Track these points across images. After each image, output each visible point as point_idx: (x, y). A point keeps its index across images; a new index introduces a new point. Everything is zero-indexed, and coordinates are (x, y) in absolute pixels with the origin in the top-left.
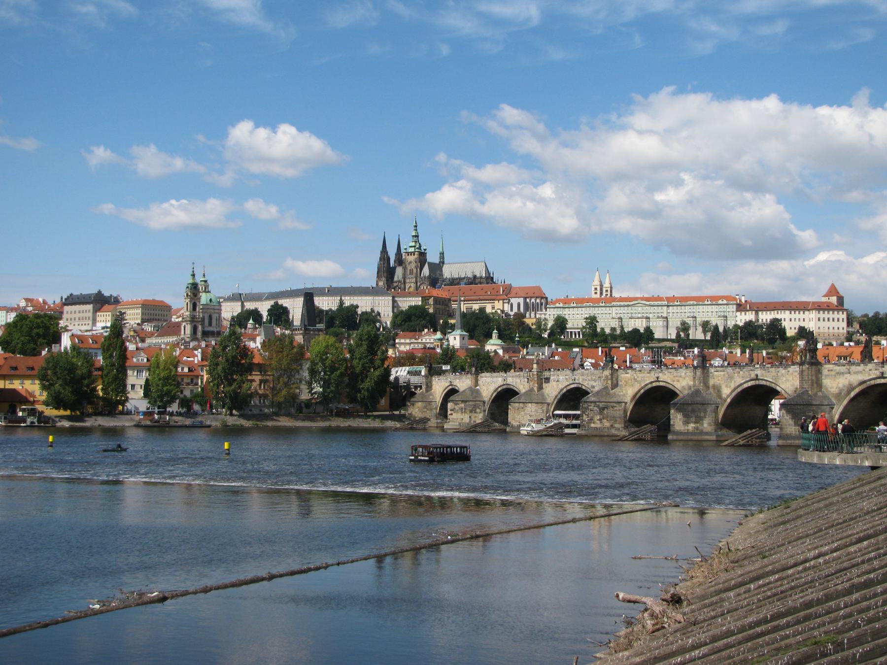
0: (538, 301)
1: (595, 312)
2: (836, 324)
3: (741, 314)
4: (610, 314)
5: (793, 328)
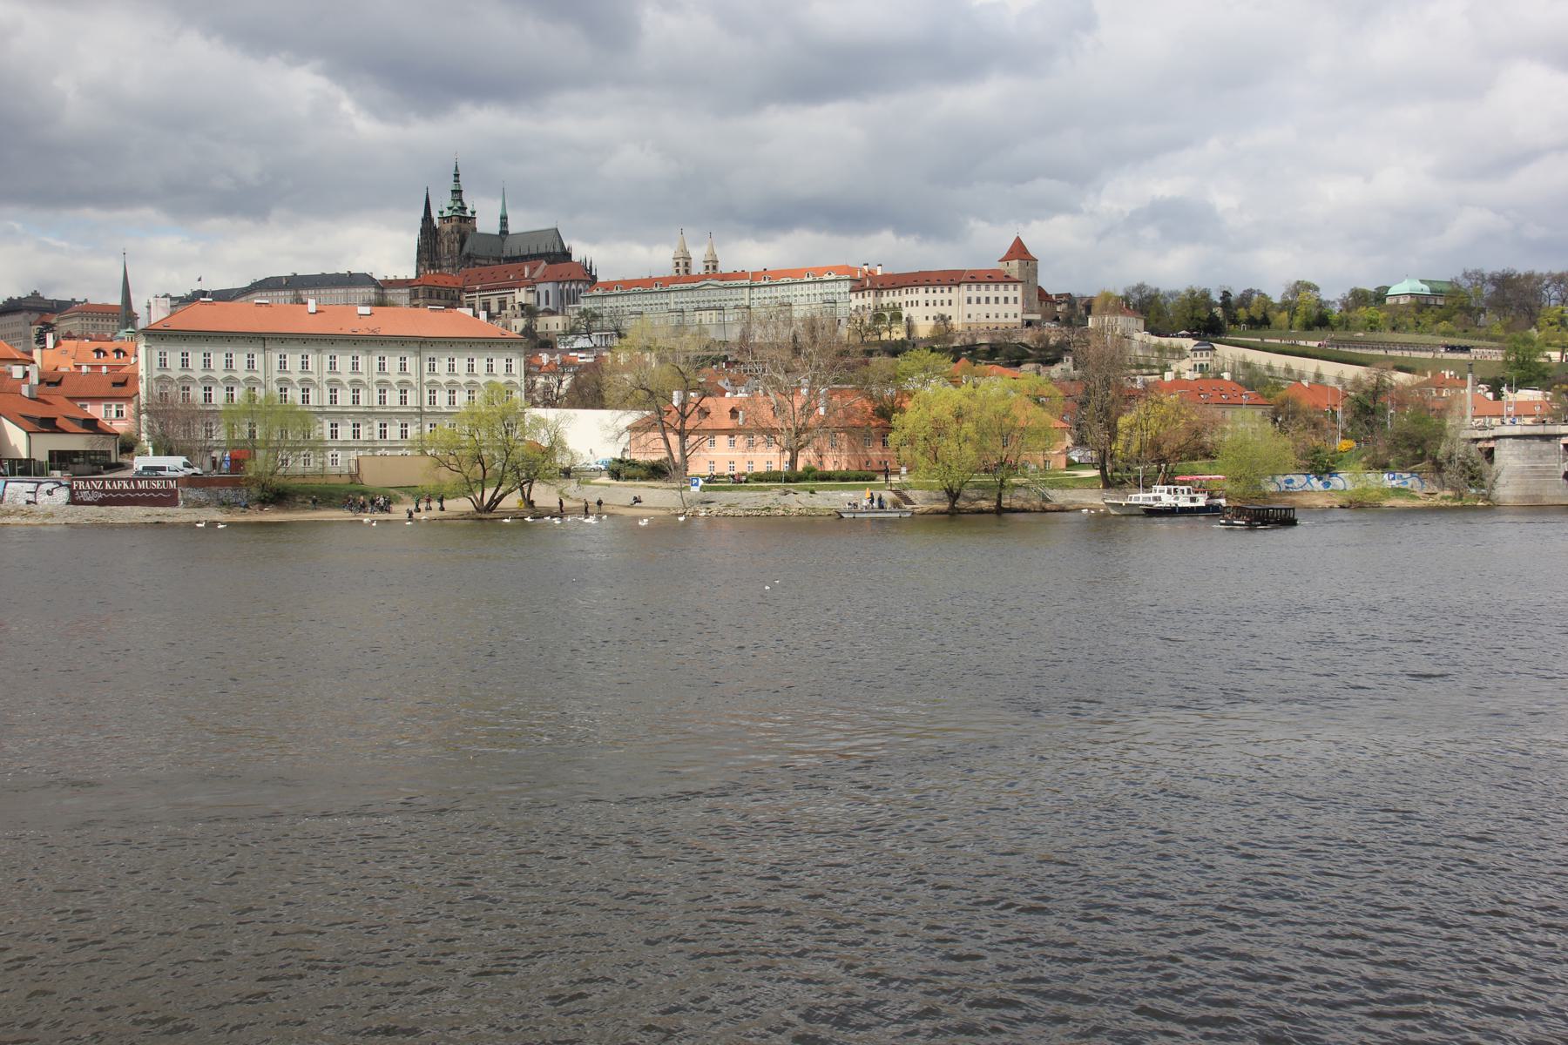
0: (573, 286)
1: (646, 302)
2: (1001, 308)
3: (857, 297)
4: (667, 304)
5: (931, 318)
